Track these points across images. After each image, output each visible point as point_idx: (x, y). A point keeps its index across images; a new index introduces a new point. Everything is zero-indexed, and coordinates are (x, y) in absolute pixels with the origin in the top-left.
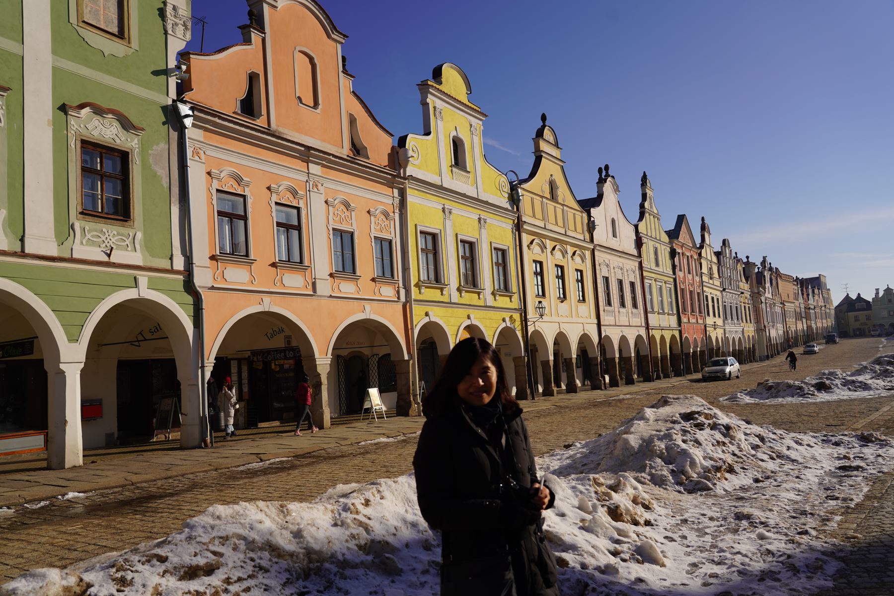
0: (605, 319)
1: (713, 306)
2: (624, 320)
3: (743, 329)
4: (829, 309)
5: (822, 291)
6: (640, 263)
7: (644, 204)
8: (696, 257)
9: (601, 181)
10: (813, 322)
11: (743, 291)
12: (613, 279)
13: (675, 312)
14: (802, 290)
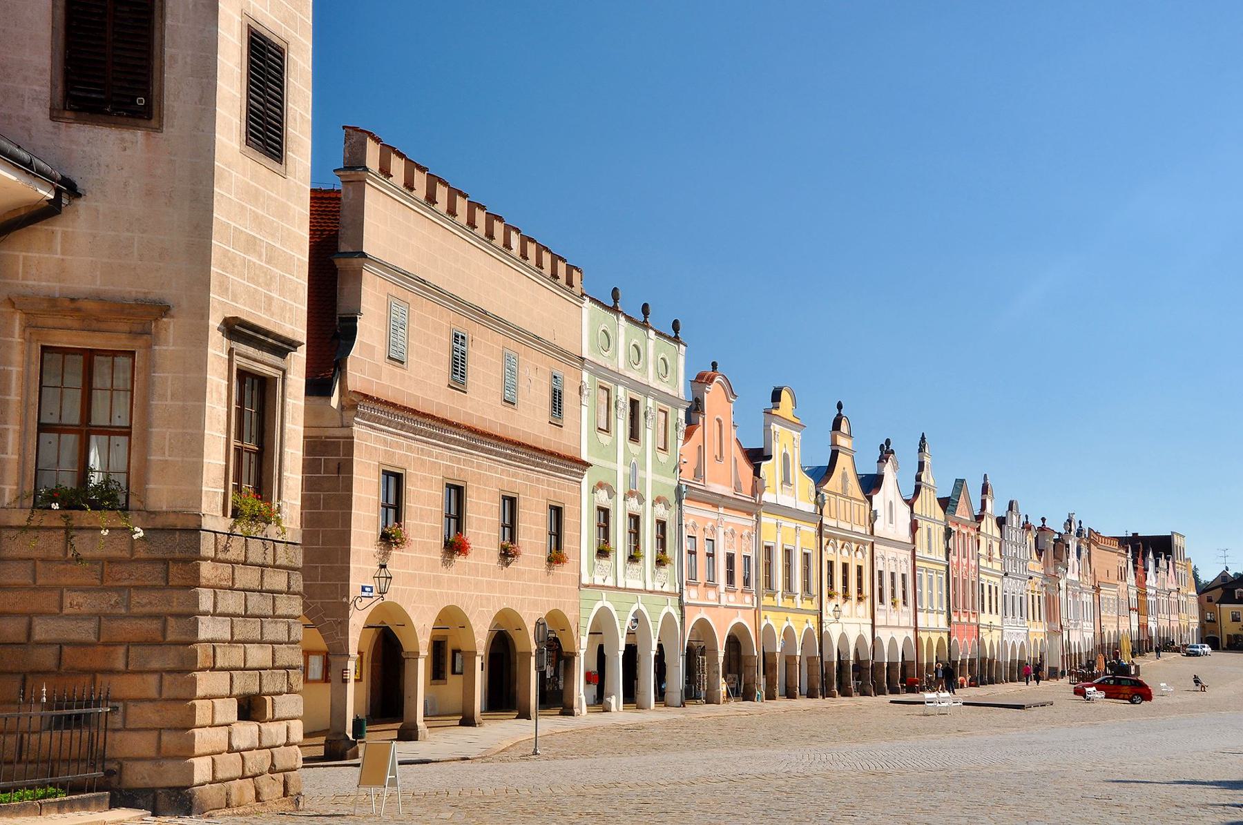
0: (880, 619)
1: (990, 598)
2: (894, 619)
3: (1028, 631)
4: (1187, 596)
5: (1174, 563)
6: (914, 551)
7: (921, 476)
8: (973, 533)
9: (883, 459)
10: (1149, 619)
11: (1032, 575)
12: (887, 572)
13: (945, 608)
14: (1135, 562)
